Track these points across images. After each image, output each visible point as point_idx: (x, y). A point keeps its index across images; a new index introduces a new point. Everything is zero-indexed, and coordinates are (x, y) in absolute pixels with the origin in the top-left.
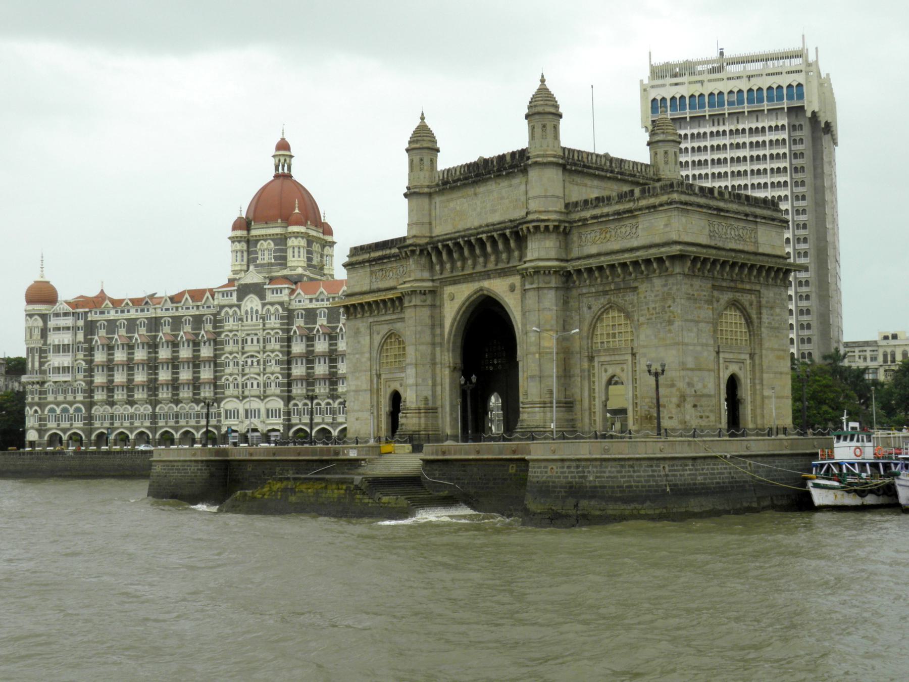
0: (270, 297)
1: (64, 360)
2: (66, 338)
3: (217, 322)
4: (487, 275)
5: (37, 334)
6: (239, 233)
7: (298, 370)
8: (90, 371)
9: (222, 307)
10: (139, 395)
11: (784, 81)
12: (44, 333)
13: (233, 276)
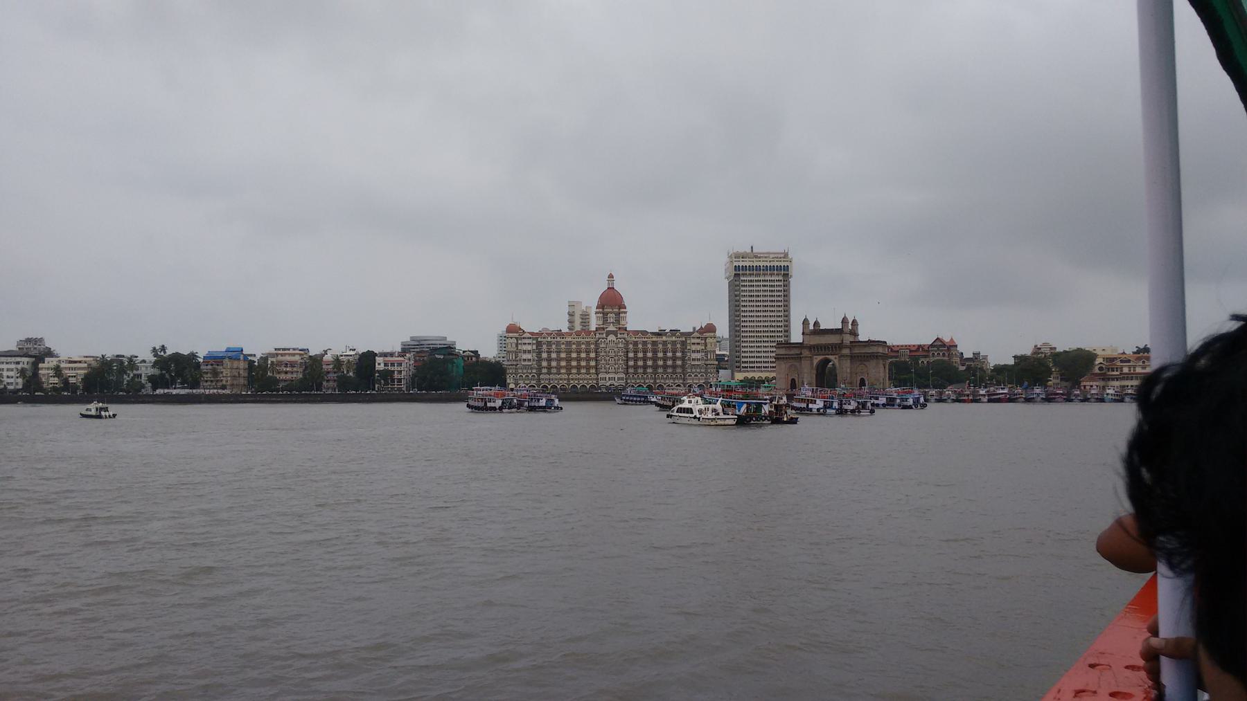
0: (619, 336)
1: (529, 356)
2: (529, 348)
3: (596, 344)
4: (828, 355)
5: (514, 345)
6: (601, 310)
7: (631, 363)
8: (540, 360)
9: (599, 339)
10: (563, 371)
11: (782, 264)
12: (517, 345)
13: (597, 326)
